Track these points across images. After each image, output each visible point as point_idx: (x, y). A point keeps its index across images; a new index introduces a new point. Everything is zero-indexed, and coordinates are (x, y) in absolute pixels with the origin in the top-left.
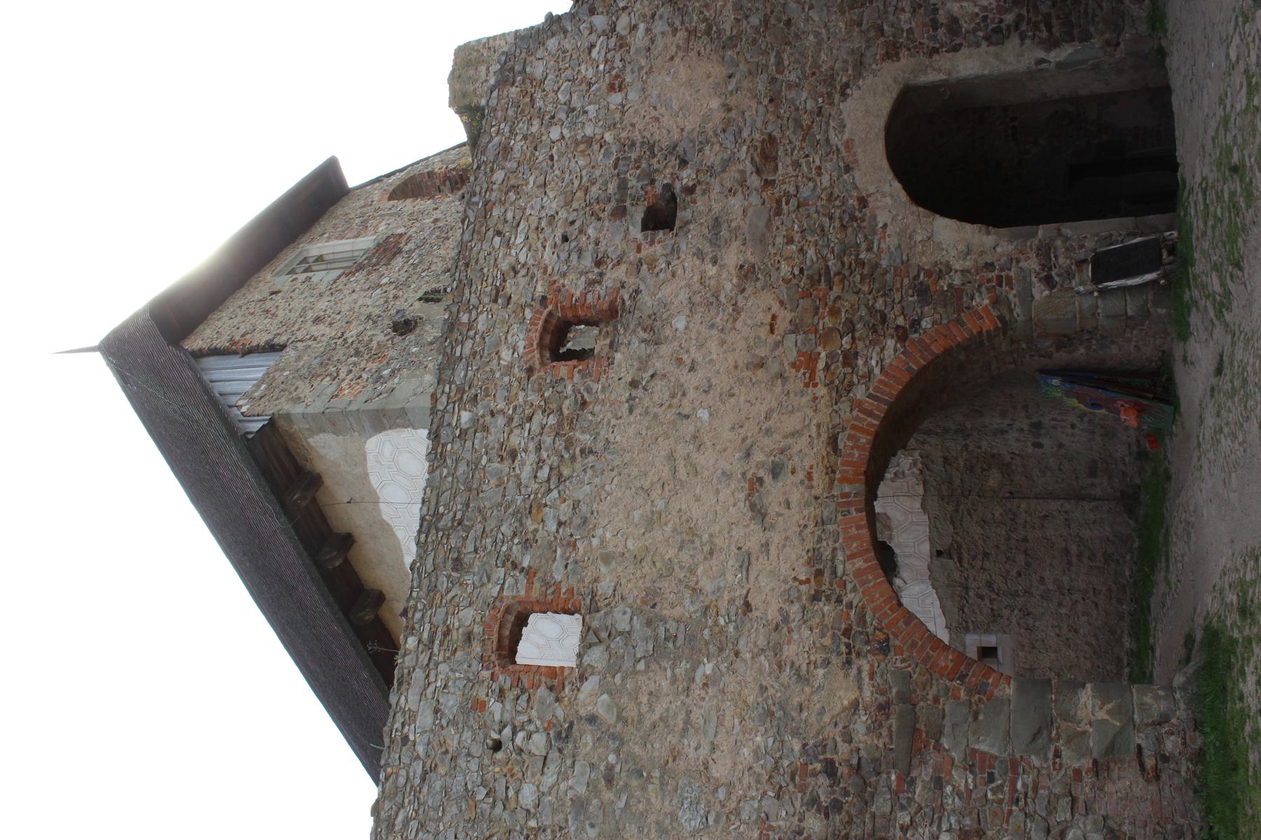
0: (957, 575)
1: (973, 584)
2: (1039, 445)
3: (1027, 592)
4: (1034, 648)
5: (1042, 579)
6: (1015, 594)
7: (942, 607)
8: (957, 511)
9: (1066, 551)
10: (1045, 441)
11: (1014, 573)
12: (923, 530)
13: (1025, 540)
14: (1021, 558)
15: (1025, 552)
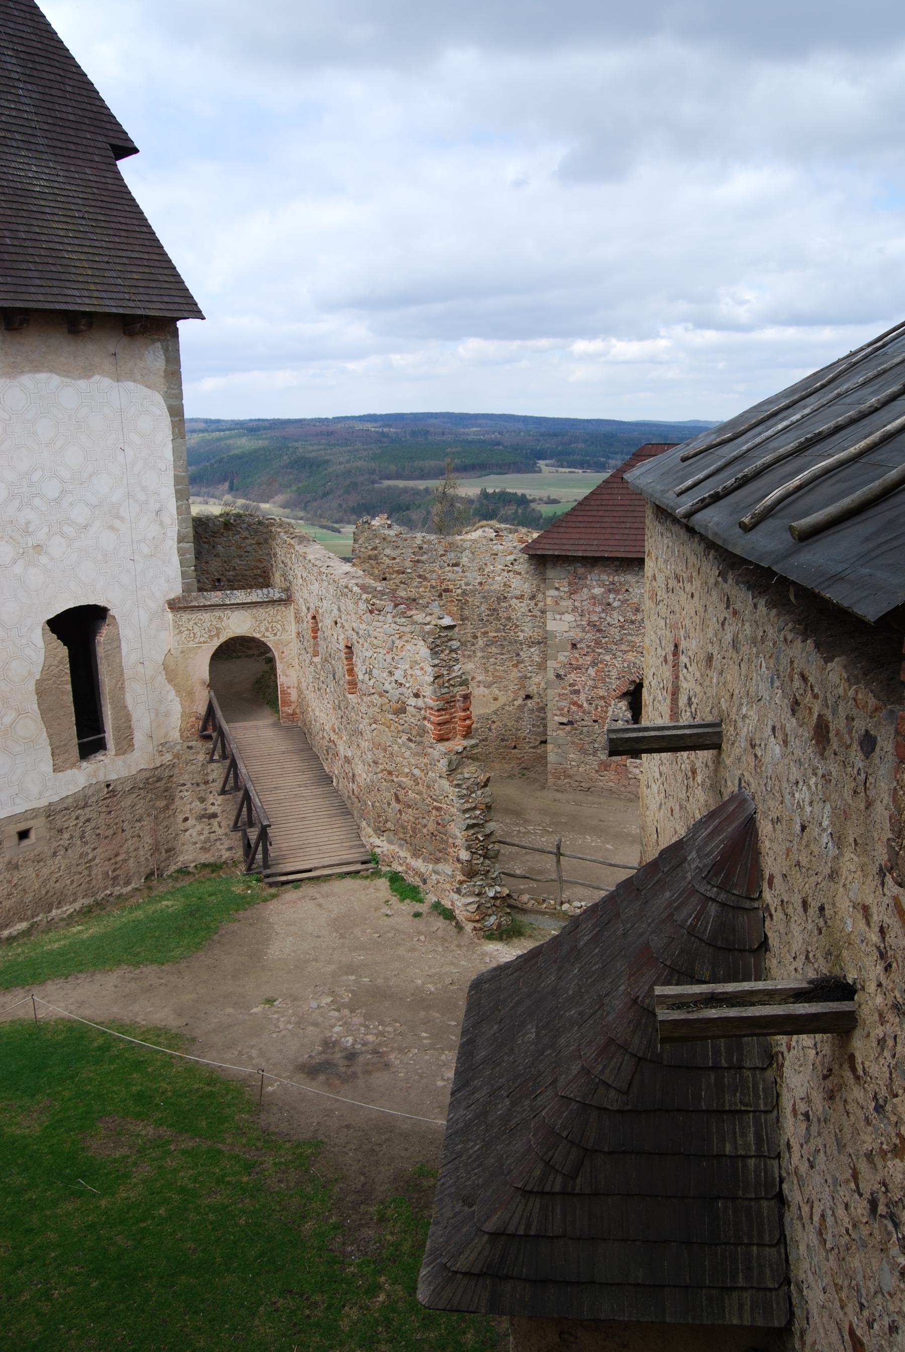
0: (93, 799)
1: (88, 810)
2: (186, 819)
3: (86, 843)
4: (38, 862)
5: (95, 849)
6: (82, 837)
7: (67, 797)
8: (140, 789)
9: (117, 855)
10: (191, 822)
11: (98, 831)
12: (124, 773)
13: (123, 831)
14: (110, 832)
15: (115, 834)
